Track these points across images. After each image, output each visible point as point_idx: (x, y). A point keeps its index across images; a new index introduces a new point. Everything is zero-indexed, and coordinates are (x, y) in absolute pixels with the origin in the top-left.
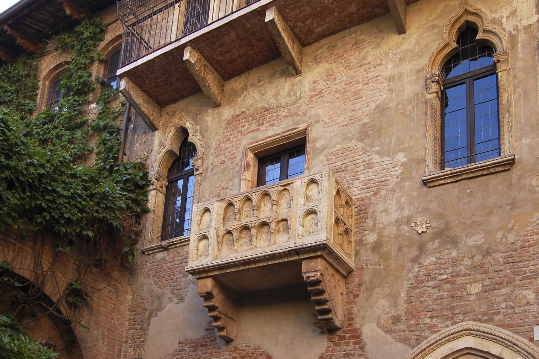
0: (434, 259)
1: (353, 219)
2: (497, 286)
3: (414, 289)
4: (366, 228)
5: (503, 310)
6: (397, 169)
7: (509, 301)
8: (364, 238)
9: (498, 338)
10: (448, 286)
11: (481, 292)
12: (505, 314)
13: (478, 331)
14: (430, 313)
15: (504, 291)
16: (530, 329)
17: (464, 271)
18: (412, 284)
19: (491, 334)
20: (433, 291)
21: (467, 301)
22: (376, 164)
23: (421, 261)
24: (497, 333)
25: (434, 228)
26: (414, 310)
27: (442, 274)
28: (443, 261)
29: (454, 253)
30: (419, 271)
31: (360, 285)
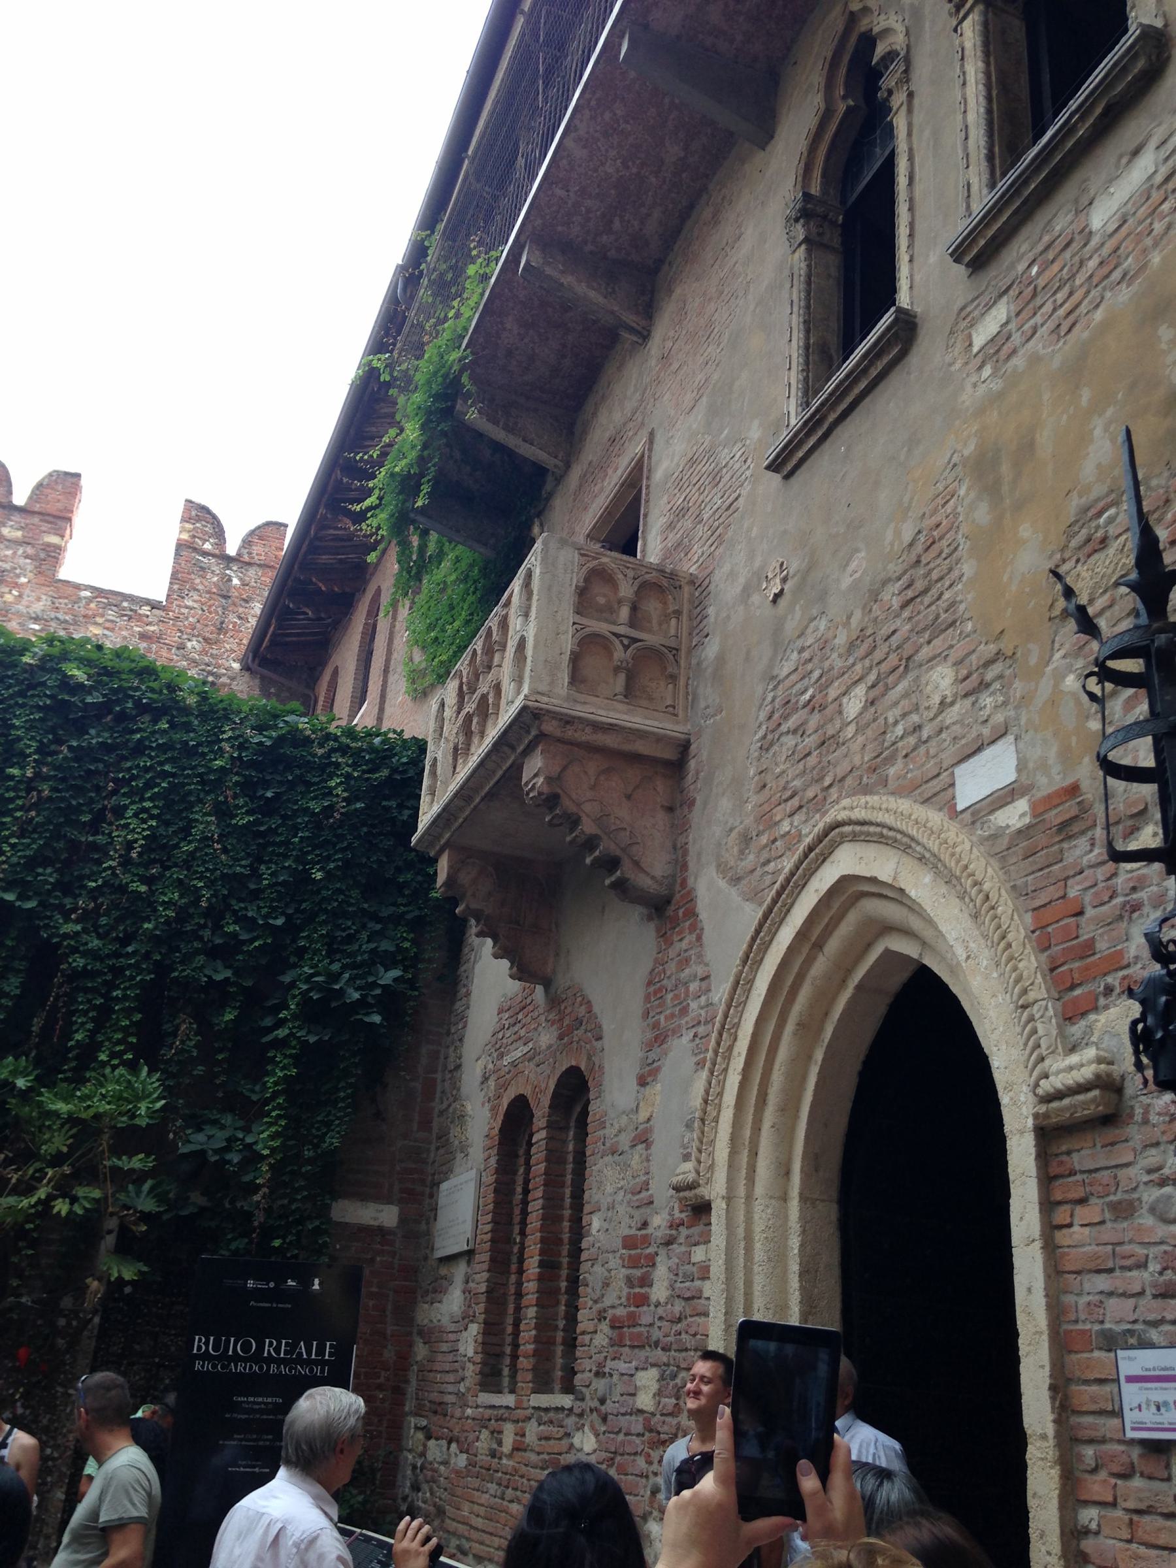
0: (795, 655)
1: (685, 618)
2: (891, 679)
3: (767, 750)
4: (706, 631)
5: (900, 744)
6: (749, 461)
7: (910, 712)
8: (703, 656)
9: (885, 831)
10: (814, 720)
11: (865, 708)
12: (904, 753)
13: (850, 822)
14: (789, 803)
15: (900, 688)
16: (948, 781)
17: (839, 664)
18: (764, 737)
19: (870, 823)
20: (790, 741)
21: (843, 744)
22: (725, 470)
23: (775, 673)
24: (880, 817)
25: (794, 575)
26: (766, 806)
27: (806, 690)
28: (806, 655)
29: (823, 624)
30: (773, 701)
31: (697, 773)
